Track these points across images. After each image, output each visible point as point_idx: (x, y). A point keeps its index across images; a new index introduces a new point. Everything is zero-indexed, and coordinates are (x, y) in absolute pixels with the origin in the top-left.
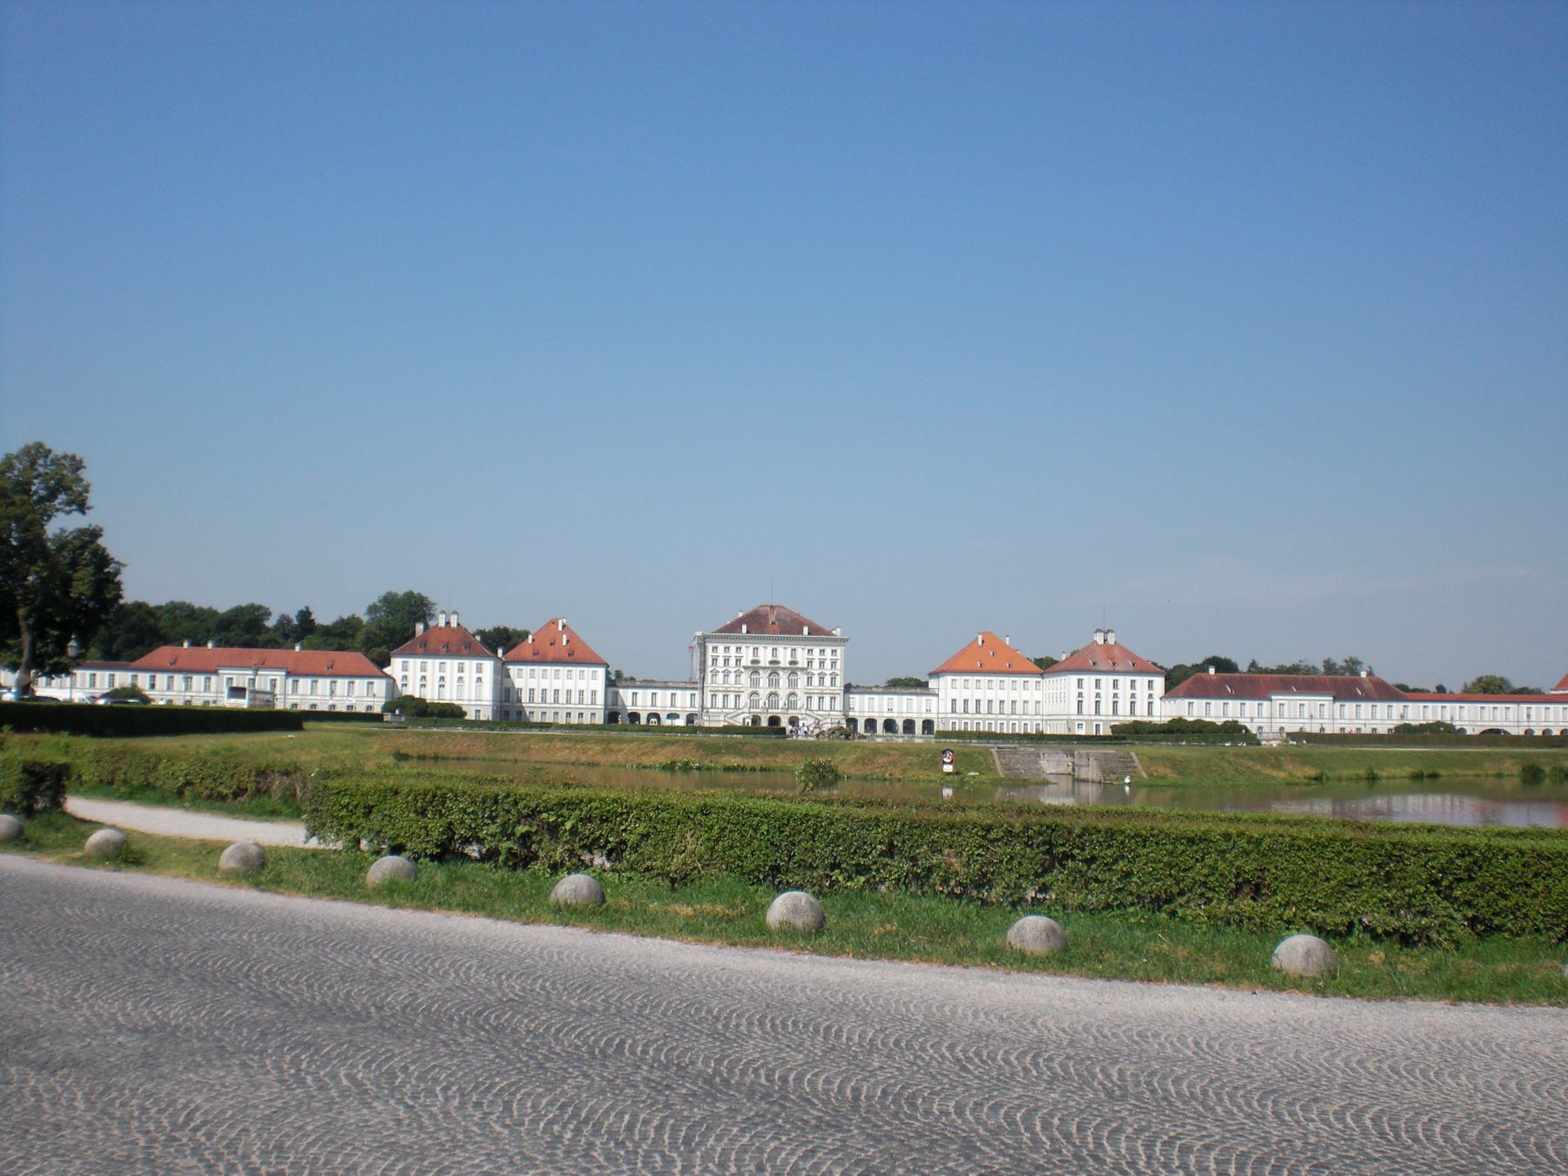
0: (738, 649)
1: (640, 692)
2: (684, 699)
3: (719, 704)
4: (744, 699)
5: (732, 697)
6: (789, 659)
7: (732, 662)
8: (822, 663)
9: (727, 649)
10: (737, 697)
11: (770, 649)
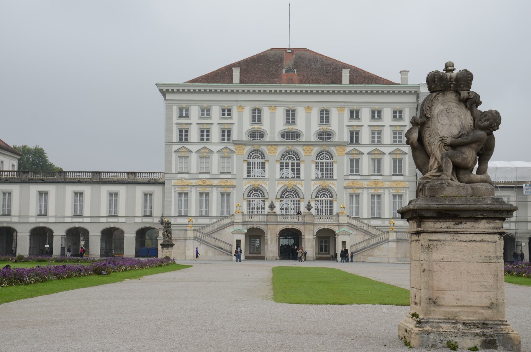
0: (226, 113)
1: (51, 189)
2: (131, 203)
3: (193, 211)
4: (239, 202)
5: (215, 197)
6: (315, 127)
7: (215, 135)
8: (376, 135)
9: (205, 113)
10: (225, 196)
11: (280, 113)
